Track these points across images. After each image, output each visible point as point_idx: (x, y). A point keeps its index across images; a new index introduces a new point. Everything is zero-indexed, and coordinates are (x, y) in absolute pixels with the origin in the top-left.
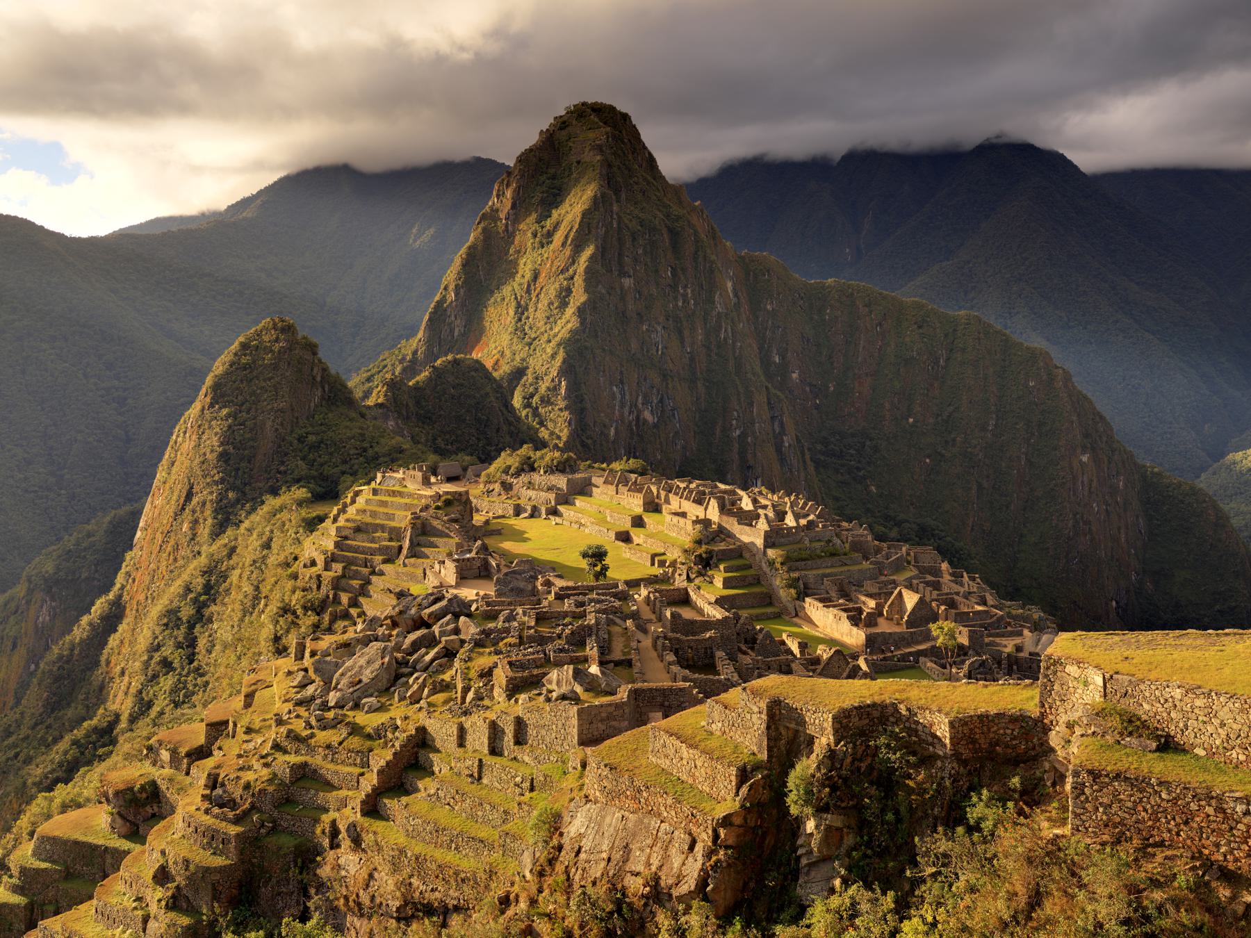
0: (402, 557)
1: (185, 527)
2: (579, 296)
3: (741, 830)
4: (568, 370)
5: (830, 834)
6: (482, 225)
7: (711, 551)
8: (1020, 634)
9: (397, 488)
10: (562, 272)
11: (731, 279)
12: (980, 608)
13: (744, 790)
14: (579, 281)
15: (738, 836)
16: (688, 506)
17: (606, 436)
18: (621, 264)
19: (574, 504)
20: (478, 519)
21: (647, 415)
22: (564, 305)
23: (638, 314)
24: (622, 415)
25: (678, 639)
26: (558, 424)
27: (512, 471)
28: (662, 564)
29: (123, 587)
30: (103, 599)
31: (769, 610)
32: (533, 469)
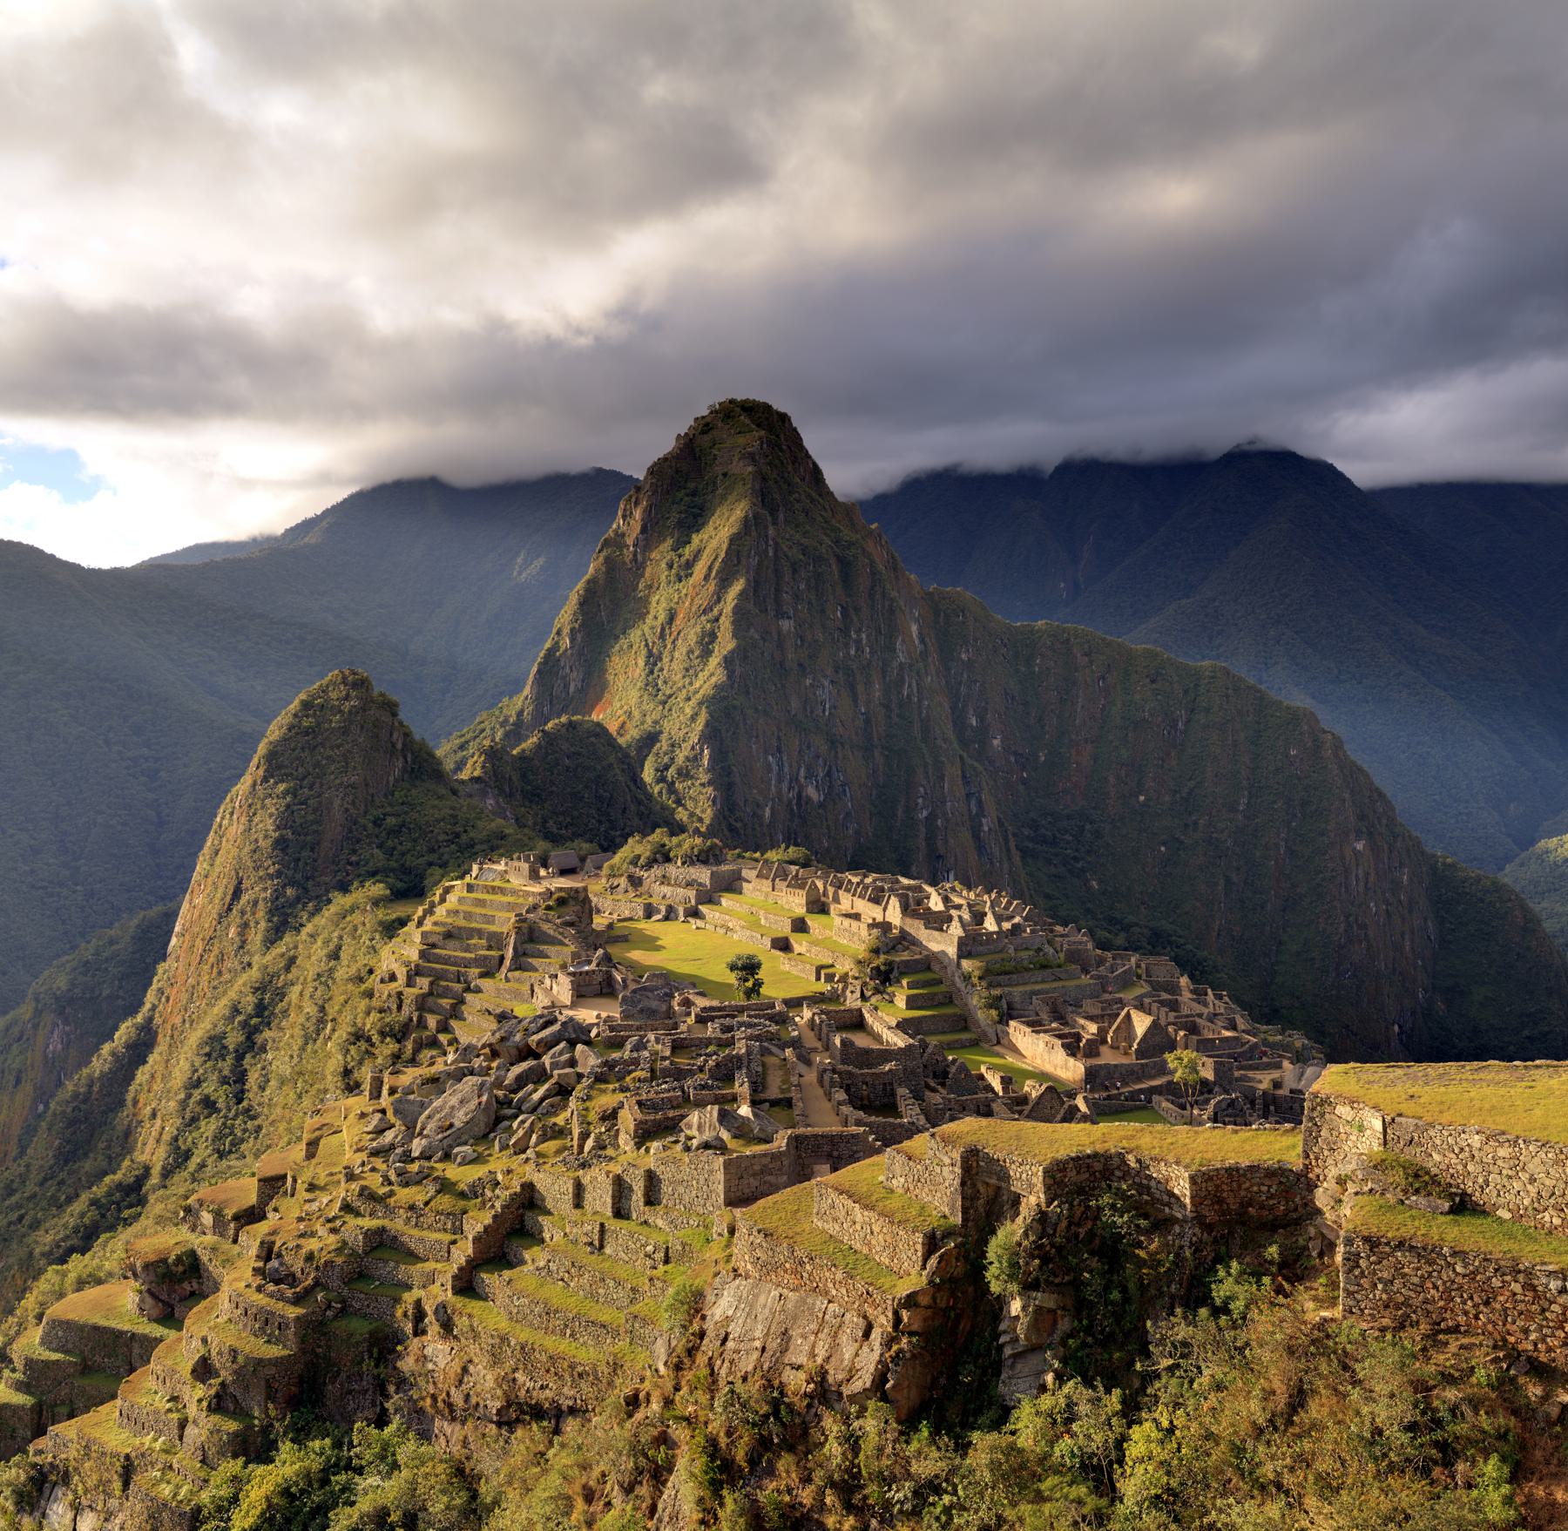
0: (504, 969)
1: (232, 932)
2: (726, 643)
3: (929, 1312)
4: (711, 735)
6: (604, 553)
7: (891, 962)
8: (1279, 1066)
9: (497, 883)
10: (705, 612)
11: (917, 621)
13: (933, 1262)
14: (726, 623)
15: (925, 1320)
16: (862, 906)
17: (760, 817)
18: (778, 602)
20: (599, 922)
21: (811, 792)
22: (706, 653)
23: (800, 665)
24: (779, 792)
25: (850, 1073)
26: (699, 803)
27: (642, 861)
28: (830, 978)
29: (154, 1008)
30: (128, 1023)
31: (965, 1036)
32: (668, 859)
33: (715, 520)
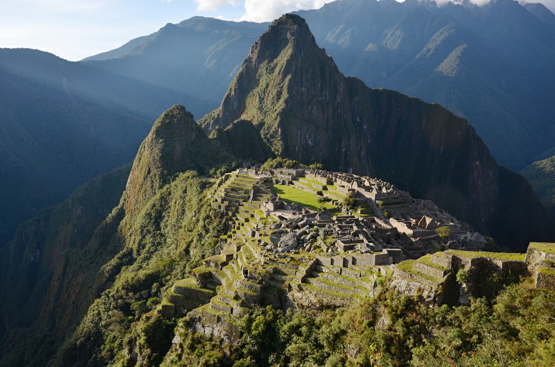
0: (250, 200)
1: (149, 183)
2: (285, 95)
4: (280, 125)
5: (469, 288)
6: (245, 64)
8: (466, 233)
9: (245, 175)
10: (278, 85)
12: (452, 224)
13: (446, 277)
17: (296, 150)
19: (298, 180)
21: (310, 142)
22: (279, 98)
27: (273, 166)
28: (337, 204)
29: (123, 204)
30: (116, 208)
32: (282, 167)
33: (282, 54)
